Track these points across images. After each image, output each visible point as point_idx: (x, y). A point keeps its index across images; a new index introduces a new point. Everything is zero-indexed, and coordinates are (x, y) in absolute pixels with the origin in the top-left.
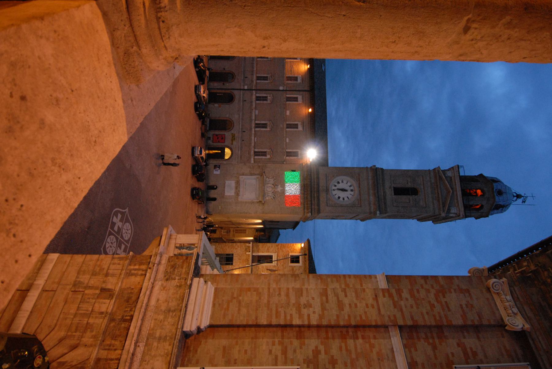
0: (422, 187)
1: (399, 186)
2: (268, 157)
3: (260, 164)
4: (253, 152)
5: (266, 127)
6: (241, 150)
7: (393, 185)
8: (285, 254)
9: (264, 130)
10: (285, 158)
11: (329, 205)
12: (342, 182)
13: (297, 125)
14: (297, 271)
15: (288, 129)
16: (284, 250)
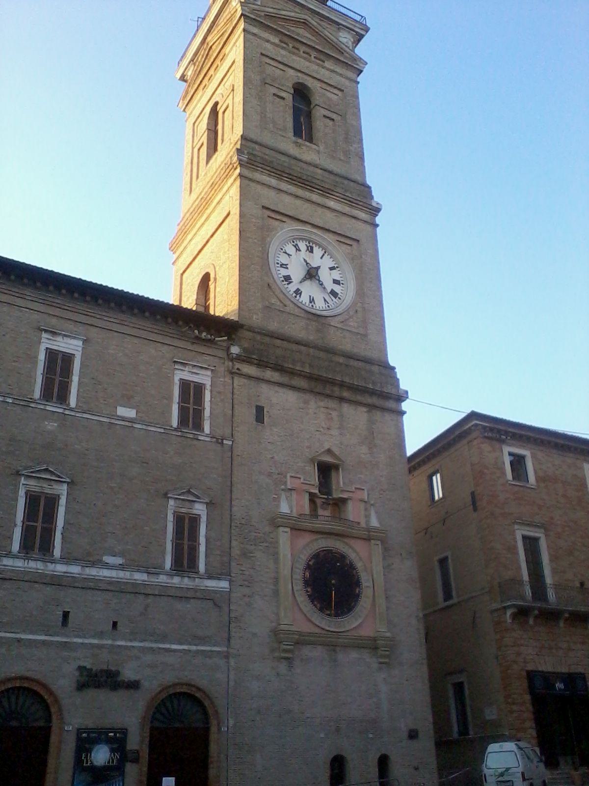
0: (291, 72)
1: (290, 124)
2: (200, 509)
3: (236, 552)
4: (176, 580)
5: (52, 502)
6: (164, 638)
7: (291, 134)
10: (208, 439)
11: (361, 331)
13: (52, 355)
15: (73, 401)
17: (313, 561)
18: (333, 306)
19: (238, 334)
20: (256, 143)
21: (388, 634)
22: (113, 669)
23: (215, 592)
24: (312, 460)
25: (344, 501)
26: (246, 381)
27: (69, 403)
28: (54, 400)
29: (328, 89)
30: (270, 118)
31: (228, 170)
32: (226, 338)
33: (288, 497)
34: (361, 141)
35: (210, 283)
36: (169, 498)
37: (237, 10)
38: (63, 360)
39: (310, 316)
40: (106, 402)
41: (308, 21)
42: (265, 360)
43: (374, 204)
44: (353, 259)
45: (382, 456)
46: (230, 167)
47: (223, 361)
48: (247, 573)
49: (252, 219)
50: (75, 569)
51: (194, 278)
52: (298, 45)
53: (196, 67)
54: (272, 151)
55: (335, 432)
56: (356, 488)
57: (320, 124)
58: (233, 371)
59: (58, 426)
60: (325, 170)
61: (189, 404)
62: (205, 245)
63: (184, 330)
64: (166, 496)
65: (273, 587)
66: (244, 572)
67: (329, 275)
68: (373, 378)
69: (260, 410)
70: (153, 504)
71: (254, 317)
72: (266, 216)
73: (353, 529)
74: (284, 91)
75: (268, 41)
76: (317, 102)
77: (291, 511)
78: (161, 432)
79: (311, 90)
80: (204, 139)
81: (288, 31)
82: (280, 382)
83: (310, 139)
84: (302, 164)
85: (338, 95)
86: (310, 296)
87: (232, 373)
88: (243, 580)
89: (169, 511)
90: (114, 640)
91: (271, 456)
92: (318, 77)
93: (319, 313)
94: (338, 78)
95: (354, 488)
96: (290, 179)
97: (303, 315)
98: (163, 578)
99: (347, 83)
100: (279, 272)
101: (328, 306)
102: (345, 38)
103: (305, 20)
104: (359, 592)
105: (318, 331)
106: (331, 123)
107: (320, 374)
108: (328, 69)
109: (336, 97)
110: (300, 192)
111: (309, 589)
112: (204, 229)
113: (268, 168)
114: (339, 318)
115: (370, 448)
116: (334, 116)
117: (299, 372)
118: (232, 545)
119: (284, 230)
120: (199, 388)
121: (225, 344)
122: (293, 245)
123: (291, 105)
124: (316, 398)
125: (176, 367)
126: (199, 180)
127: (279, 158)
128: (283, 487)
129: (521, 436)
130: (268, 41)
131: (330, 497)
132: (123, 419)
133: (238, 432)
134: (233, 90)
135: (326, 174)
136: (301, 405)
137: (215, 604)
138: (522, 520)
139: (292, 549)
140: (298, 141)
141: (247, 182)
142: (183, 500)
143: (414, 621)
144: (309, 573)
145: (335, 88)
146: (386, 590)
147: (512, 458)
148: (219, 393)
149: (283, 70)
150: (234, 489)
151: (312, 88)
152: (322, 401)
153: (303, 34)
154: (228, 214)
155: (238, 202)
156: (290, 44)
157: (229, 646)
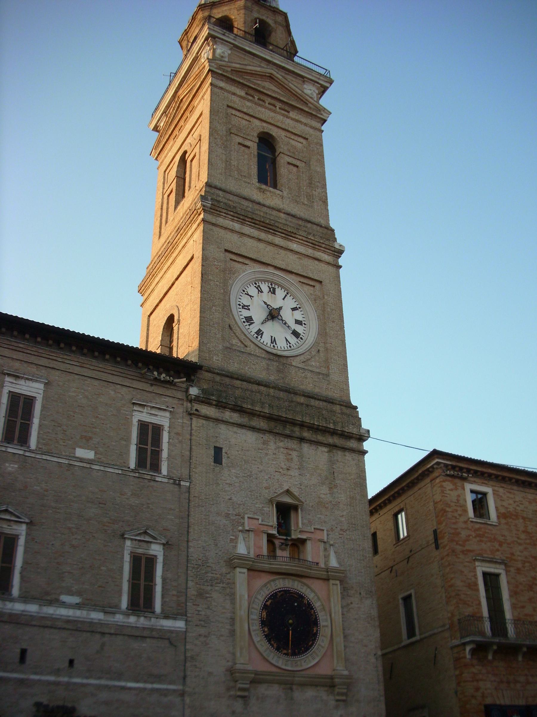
0: (257, 122)
1: (254, 170)
2: (156, 550)
3: (192, 592)
4: (132, 619)
6: (119, 676)
7: (255, 180)
8: (474, 534)
9: (26, 552)
10: (166, 480)
11: (324, 371)
12: (246, 307)
14: (504, 504)
15: (33, 442)
16: (464, 534)
17: (270, 601)
18: (295, 345)
19: (198, 376)
20: (220, 189)
21: (346, 673)
22: (70, 705)
23: (171, 632)
24: (271, 501)
25: (303, 542)
26: (204, 422)
27: (29, 445)
28: (16, 442)
29: (292, 137)
30: (235, 166)
31: (192, 216)
32: (185, 379)
33: (246, 538)
34: (324, 186)
35: (174, 325)
36: (125, 538)
37: (205, 66)
38: (24, 403)
39: (272, 357)
40: (64, 444)
41: (273, 75)
42: (224, 401)
43: (337, 246)
44: (315, 300)
45: (342, 496)
46: (192, 213)
47: (181, 402)
48: (203, 613)
49: (215, 262)
50: (32, 608)
51: (160, 320)
52: (262, 97)
53: (168, 118)
54: (235, 197)
55: (294, 473)
56: (314, 529)
57: (283, 170)
58: (192, 412)
59: (19, 468)
60: (288, 214)
61: (147, 446)
62: (170, 288)
63: (143, 371)
64: (122, 537)
65: (228, 627)
66: (201, 613)
67: (291, 315)
68: (334, 418)
69: (218, 451)
70: (110, 544)
71: (214, 357)
72: (228, 259)
73: (311, 569)
74: (249, 140)
75: (234, 94)
76: (282, 150)
77: (249, 553)
78: (119, 473)
79: (276, 139)
80: (174, 185)
81: (254, 85)
82: (238, 422)
83: (275, 186)
84: (265, 208)
85: (302, 143)
86: (272, 337)
87: (190, 414)
88: (200, 620)
89: (125, 552)
90: (70, 677)
92: (283, 127)
93: (279, 353)
94: (303, 127)
95: (313, 529)
96: (253, 223)
97: (263, 356)
98: (119, 618)
99: (311, 131)
100: (240, 313)
101: (290, 347)
102: (310, 90)
103: (271, 74)
104: (317, 631)
105: (279, 371)
106: (295, 169)
107: (280, 414)
108: (292, 119)
109: (299, 144)
110: (263, 236)
111: (266, 629)
112: (171, 270)
113: (232, 213)
114: (302, 358)
115: (331, 488)
116: (298, 163)
117: (258, 413)
118: (188, 586)
119: (246, 273)
120: (157, 429)
121: (184, 386)
122: (255, 287)
123: (256, 153)
124: (275, 439)
125: (135, 408)
126: (167, 225)
127: (243, 203)
128: (240, 528)
129: (483, 474)
130: (234, 94)
131: (289, 538)
132: (81, 460)
133: (196, 473)
134: (200, 140)
135: (290, 218)
136: (261, 446)
137: (171, 643)
138: (483, 557)
139: (249, 590)
140: (262, 187)
141: (211, 227)
142: (140, 541)
143: (373, 660)
144: (266, 614)
145: (299, 136)
146: (344, 630)
147: (474, 496)
148: (178, 434)
149: (248, 121)
150: (191, 530)
151: (277, 137)
152: (282, 441)
153: (269, 87)
154: (192, 258)
155: (201, 246)
156: (256, 97)
157: (184, 684)
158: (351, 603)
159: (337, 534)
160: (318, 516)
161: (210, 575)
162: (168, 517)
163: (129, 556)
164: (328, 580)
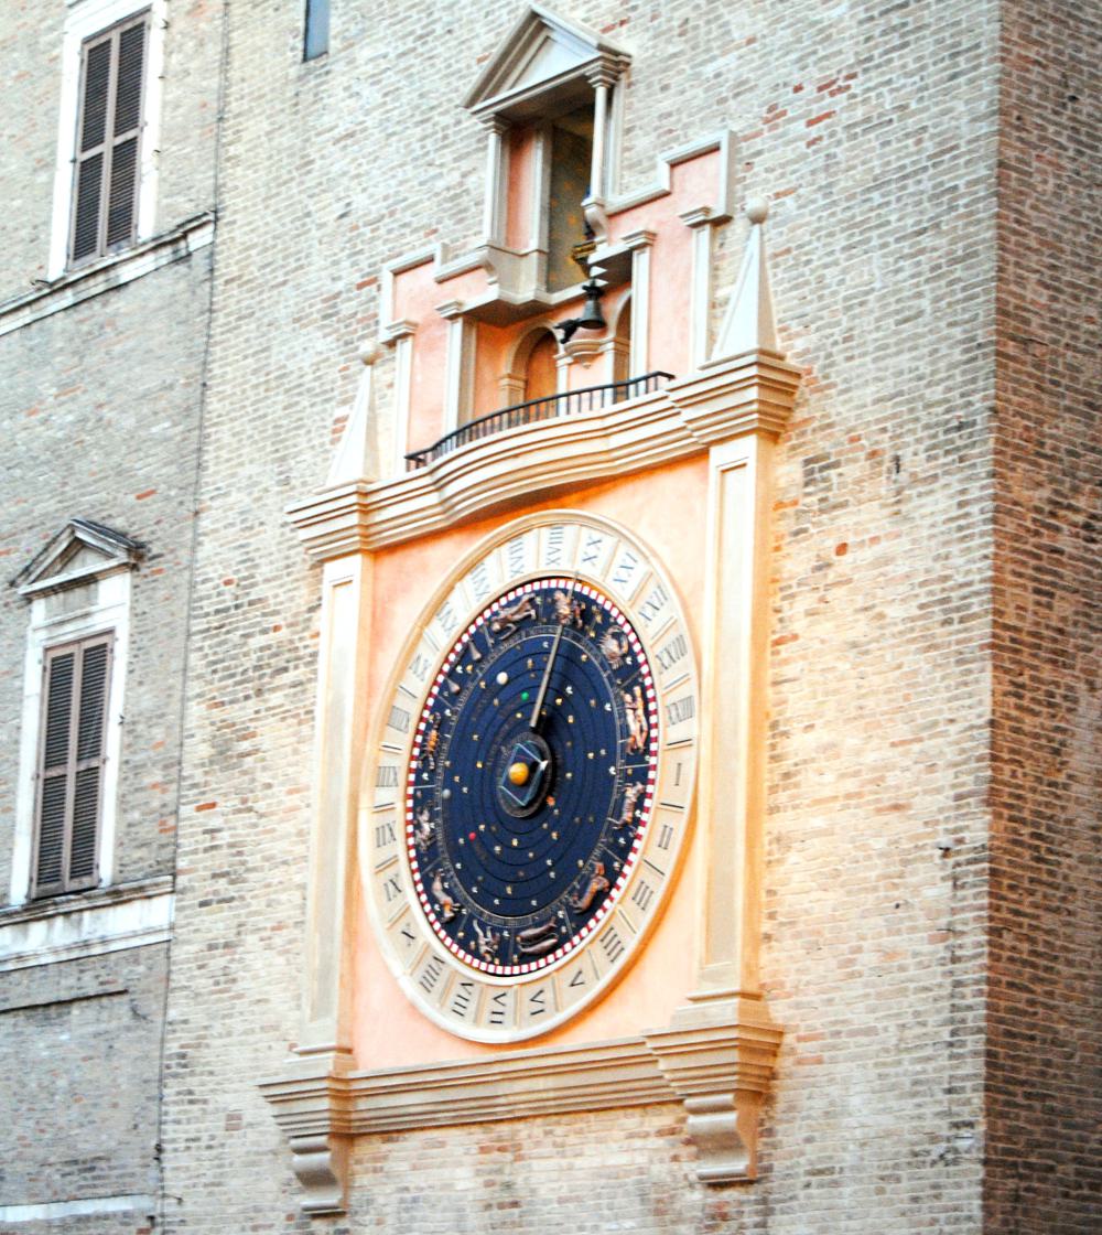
91: (339, 208)
142: (54, 590)
158: (842, 549)
159: (800, 126)
160: (709, 70)
161: (257, 641)
162: (154, 430)
163: (40, 667)
164: (701, 455)
